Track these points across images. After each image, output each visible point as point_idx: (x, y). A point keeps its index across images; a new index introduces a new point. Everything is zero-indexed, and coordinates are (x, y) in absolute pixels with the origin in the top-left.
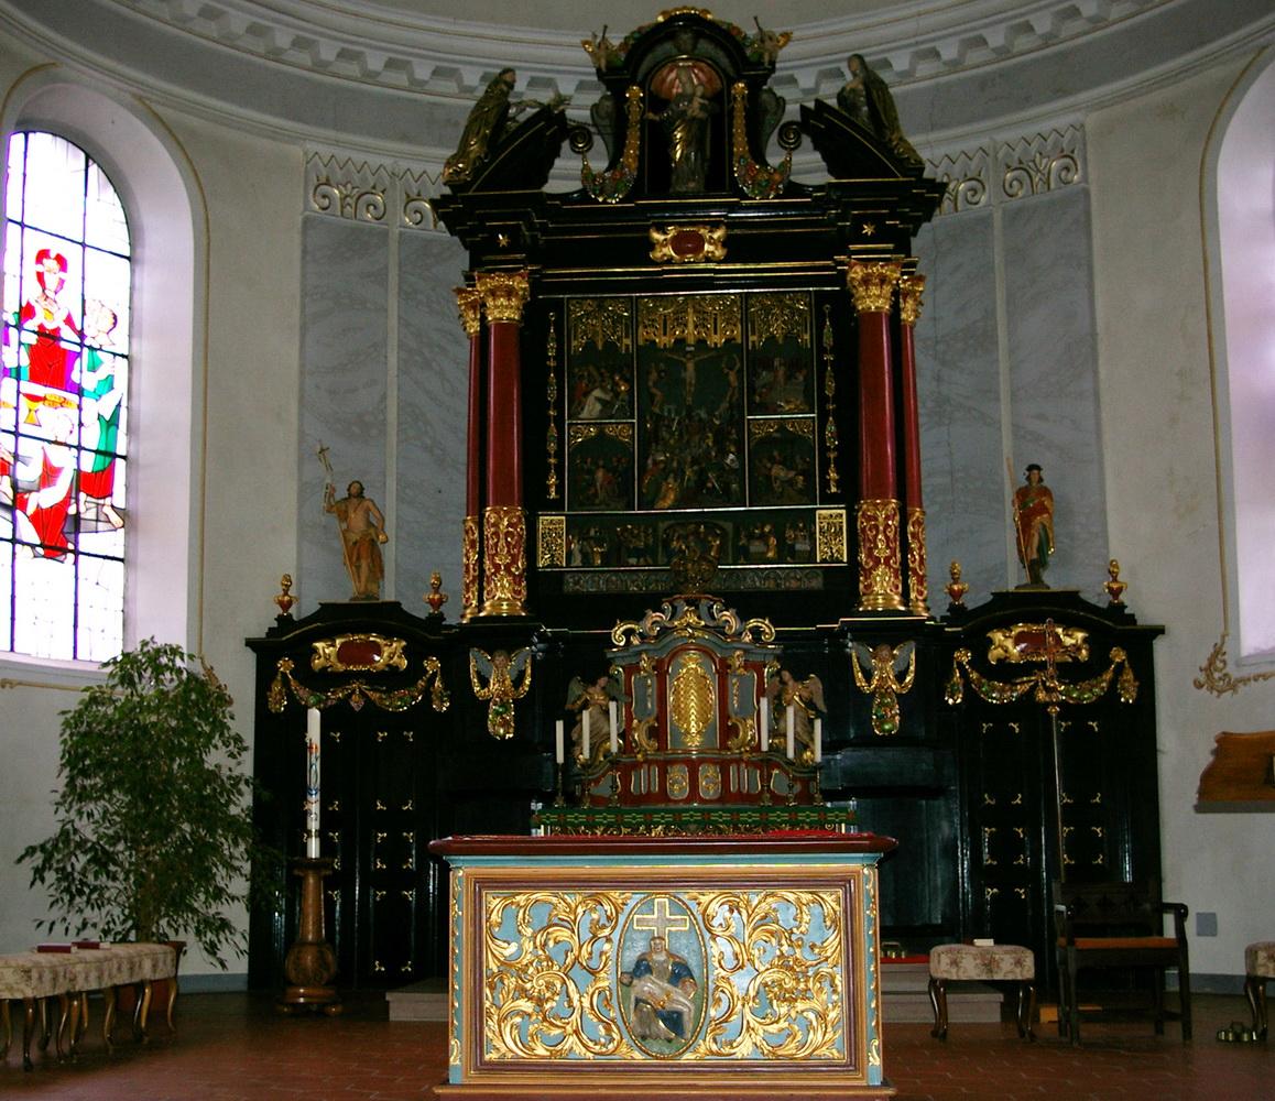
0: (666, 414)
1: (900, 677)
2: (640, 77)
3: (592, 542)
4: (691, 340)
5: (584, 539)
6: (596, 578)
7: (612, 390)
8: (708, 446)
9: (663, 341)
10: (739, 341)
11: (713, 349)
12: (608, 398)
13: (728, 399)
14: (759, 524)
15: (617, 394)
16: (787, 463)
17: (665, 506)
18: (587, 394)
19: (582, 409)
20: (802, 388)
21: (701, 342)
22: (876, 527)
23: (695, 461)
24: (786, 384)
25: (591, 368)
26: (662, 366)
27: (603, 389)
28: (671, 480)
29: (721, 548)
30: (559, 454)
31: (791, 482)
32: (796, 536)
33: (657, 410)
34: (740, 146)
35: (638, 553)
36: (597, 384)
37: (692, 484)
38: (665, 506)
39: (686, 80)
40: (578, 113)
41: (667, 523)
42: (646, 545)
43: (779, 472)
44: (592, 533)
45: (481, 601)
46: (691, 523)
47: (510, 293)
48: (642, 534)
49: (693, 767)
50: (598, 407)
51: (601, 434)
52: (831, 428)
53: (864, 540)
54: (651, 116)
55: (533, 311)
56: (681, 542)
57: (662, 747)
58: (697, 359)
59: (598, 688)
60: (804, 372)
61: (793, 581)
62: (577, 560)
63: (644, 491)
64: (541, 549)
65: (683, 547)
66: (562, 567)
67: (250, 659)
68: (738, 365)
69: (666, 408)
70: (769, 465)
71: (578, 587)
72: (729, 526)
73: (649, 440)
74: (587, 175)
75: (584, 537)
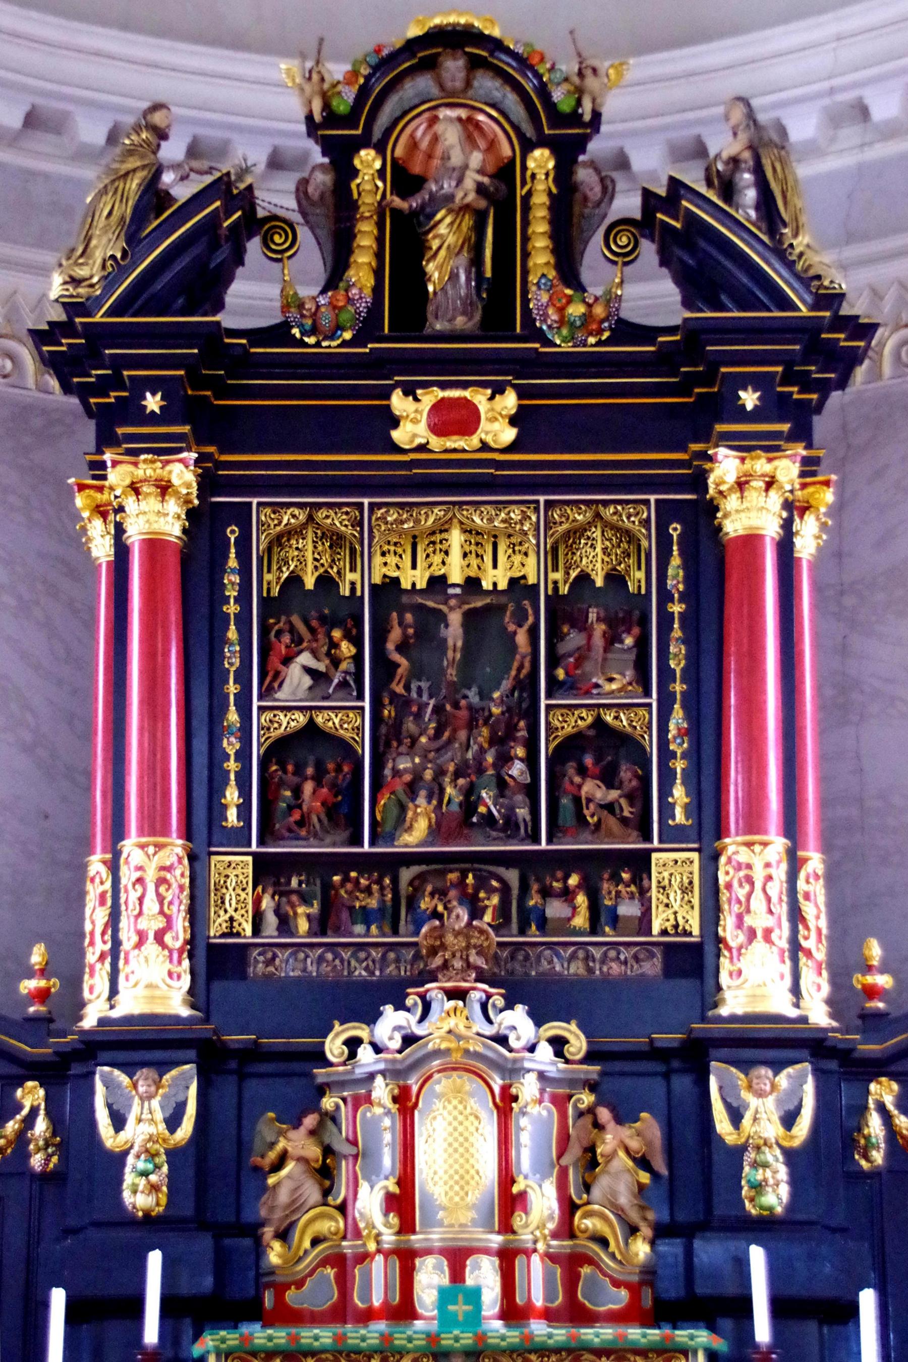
0: (414, 695)
1: (789, 1120)
2: (377, 134)
3: (294, 898)
4: (456, 577)
5: (282, 894)
6: (301, 955)
7: (328, 654)
8: (481, 747)
9: (414, 577)
10: (532, 580)
11: (488, 592)
12: (321, 667)
13: (513, 673)
14: (559, 874)
15: (336, 662)
16: (609, 779)
17: (415, 836)
18: (287, 660)
19: (280, 685)
20: (632, 656)
21: (472, 584)
22: (750, 880)
23: (457, 775)
24: (606, 650)
25: (296, 620)
26: (409, 617)
27: (315, 654)
28: (421, 800)
29: (503, 911)
30: (244, 755)
31: (610, 807)
32: (618, 893)
33: (399, 689)
34: (541, 258)
35: (366, 916)
36: (305, 644)
37: (455, 808)
38: (415, 836)
39: (455, 146)
40: (277, 197)
41: (415, 870)
42: (382, 902)
43: (592, 789)
44: (294, 882)
45: (114, 991)
46: (451, 871)
47: (164, 488)
48: (375, 887)
49: (457, 1259)
50: (307, 681)
51: (311, 722)
52: (677, 719)
53: (729, 901)
54: (398, 202)
55: (204, 521)
56: (435, 901)
57: (407, 1226)
58: (467, 607)
59: (303, 1130)
60: (636, 630)
61: (614, 965)
62: (271, 920)
63: (379, 818)
64: (212, 910)
65: (440, 908)
66: (245, 937)
68: (531, 620)
69: (414, 686)
70: (577, 779)
71: (271, 969)
72: (512, 876)
73: (386, 738)
74: (292, 303)
75: (282, 892)
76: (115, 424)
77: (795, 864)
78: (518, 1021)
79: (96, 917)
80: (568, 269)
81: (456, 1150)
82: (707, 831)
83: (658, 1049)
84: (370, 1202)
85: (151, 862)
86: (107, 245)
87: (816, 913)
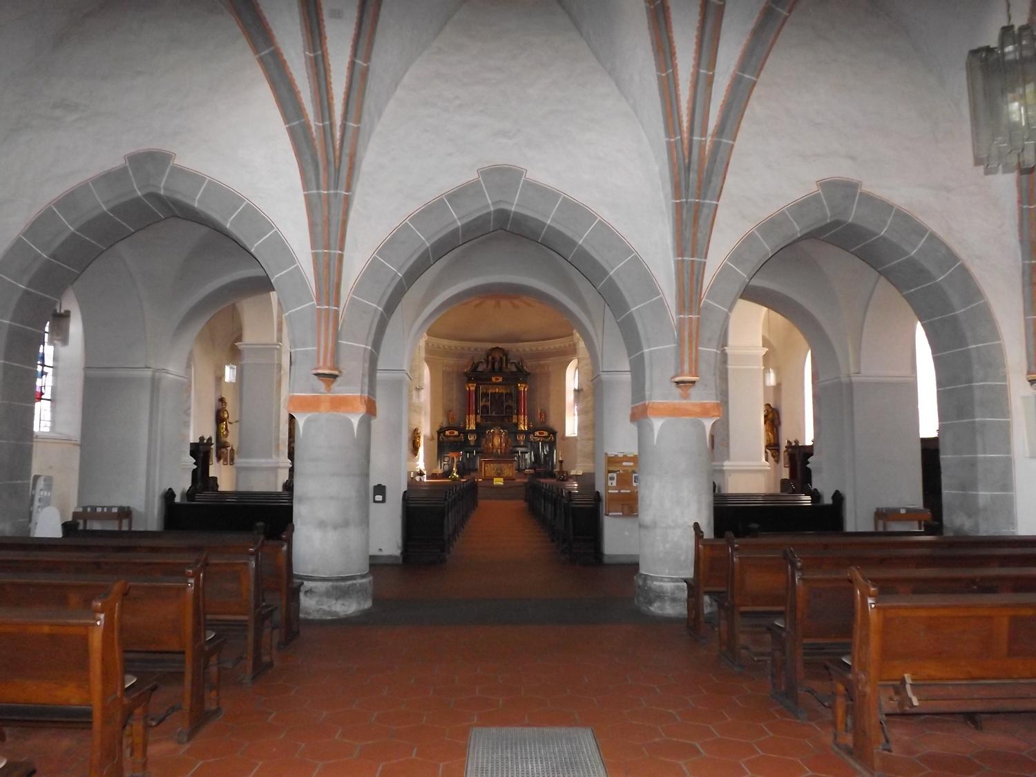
39: (497, 356)
55: (477, 388)
67: (436, 434)
76: (469, 381)
77: (524, 417)
78: (502, 431)
79: (467, 421)
80: (506, 365)
81: (497, 441)
82: (518, 414)
83: (513, 431)
84: (490, 445)
85: (472, 417)
86: (470, 368)
87: (526, 421)
